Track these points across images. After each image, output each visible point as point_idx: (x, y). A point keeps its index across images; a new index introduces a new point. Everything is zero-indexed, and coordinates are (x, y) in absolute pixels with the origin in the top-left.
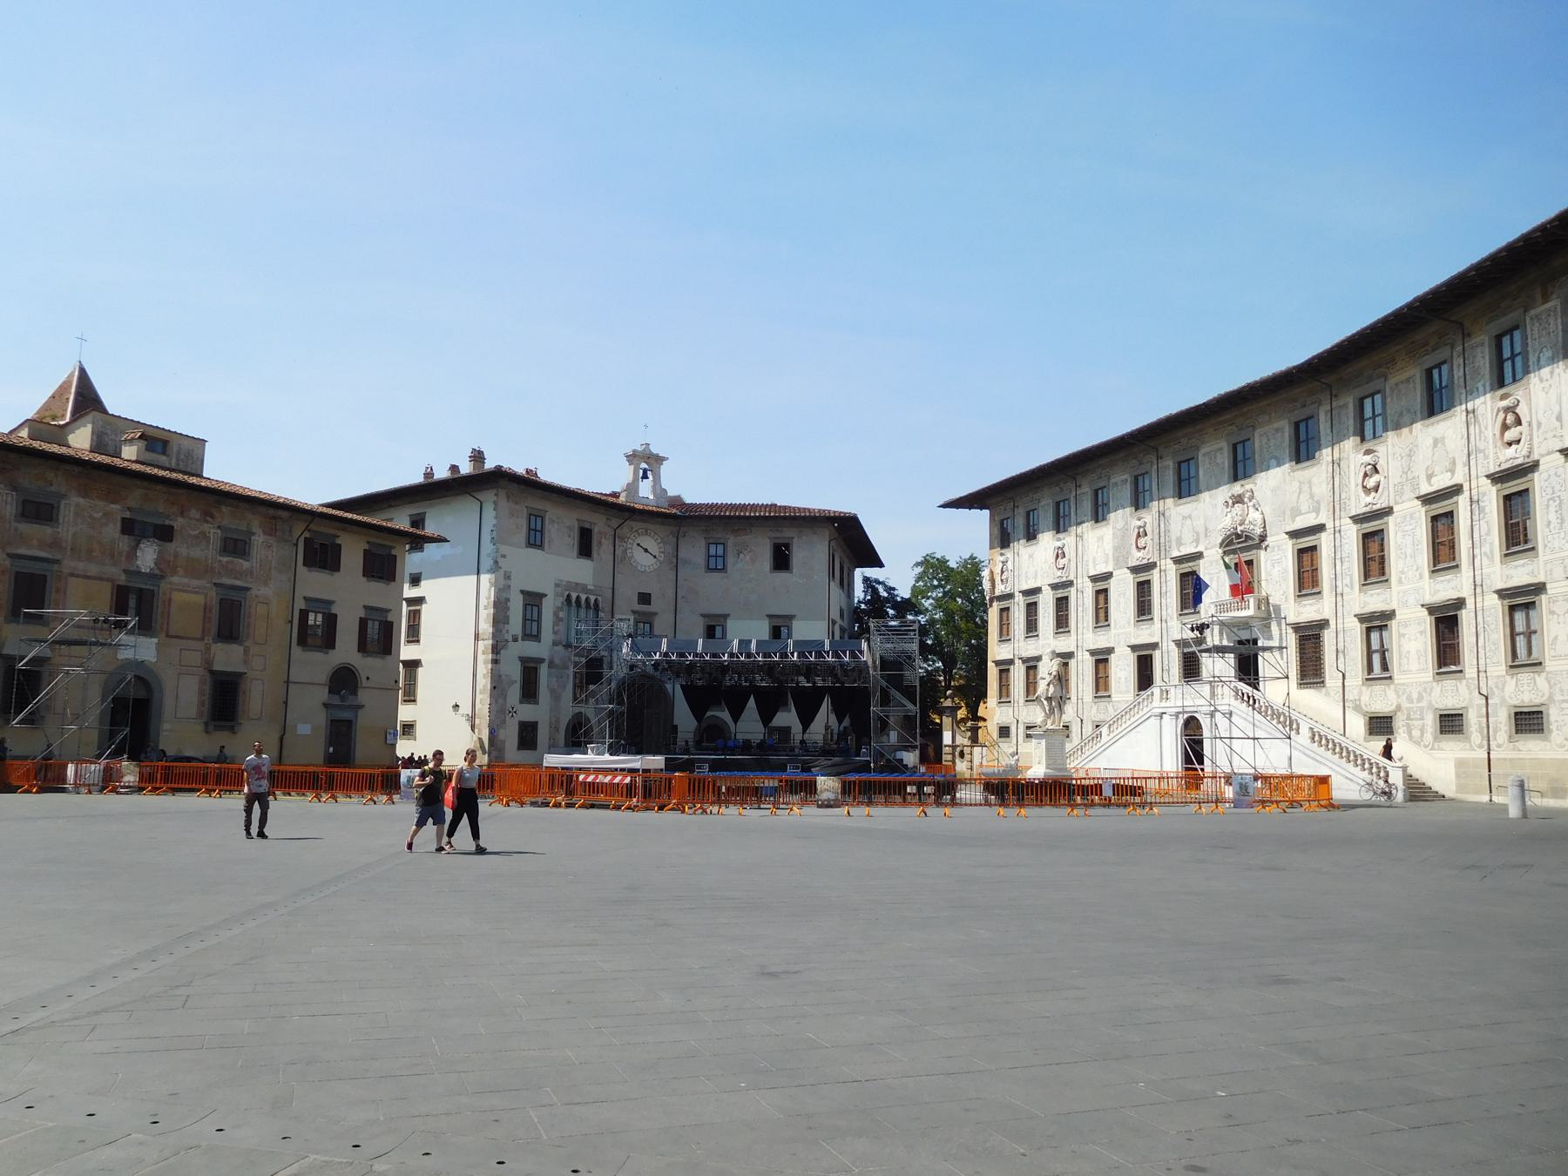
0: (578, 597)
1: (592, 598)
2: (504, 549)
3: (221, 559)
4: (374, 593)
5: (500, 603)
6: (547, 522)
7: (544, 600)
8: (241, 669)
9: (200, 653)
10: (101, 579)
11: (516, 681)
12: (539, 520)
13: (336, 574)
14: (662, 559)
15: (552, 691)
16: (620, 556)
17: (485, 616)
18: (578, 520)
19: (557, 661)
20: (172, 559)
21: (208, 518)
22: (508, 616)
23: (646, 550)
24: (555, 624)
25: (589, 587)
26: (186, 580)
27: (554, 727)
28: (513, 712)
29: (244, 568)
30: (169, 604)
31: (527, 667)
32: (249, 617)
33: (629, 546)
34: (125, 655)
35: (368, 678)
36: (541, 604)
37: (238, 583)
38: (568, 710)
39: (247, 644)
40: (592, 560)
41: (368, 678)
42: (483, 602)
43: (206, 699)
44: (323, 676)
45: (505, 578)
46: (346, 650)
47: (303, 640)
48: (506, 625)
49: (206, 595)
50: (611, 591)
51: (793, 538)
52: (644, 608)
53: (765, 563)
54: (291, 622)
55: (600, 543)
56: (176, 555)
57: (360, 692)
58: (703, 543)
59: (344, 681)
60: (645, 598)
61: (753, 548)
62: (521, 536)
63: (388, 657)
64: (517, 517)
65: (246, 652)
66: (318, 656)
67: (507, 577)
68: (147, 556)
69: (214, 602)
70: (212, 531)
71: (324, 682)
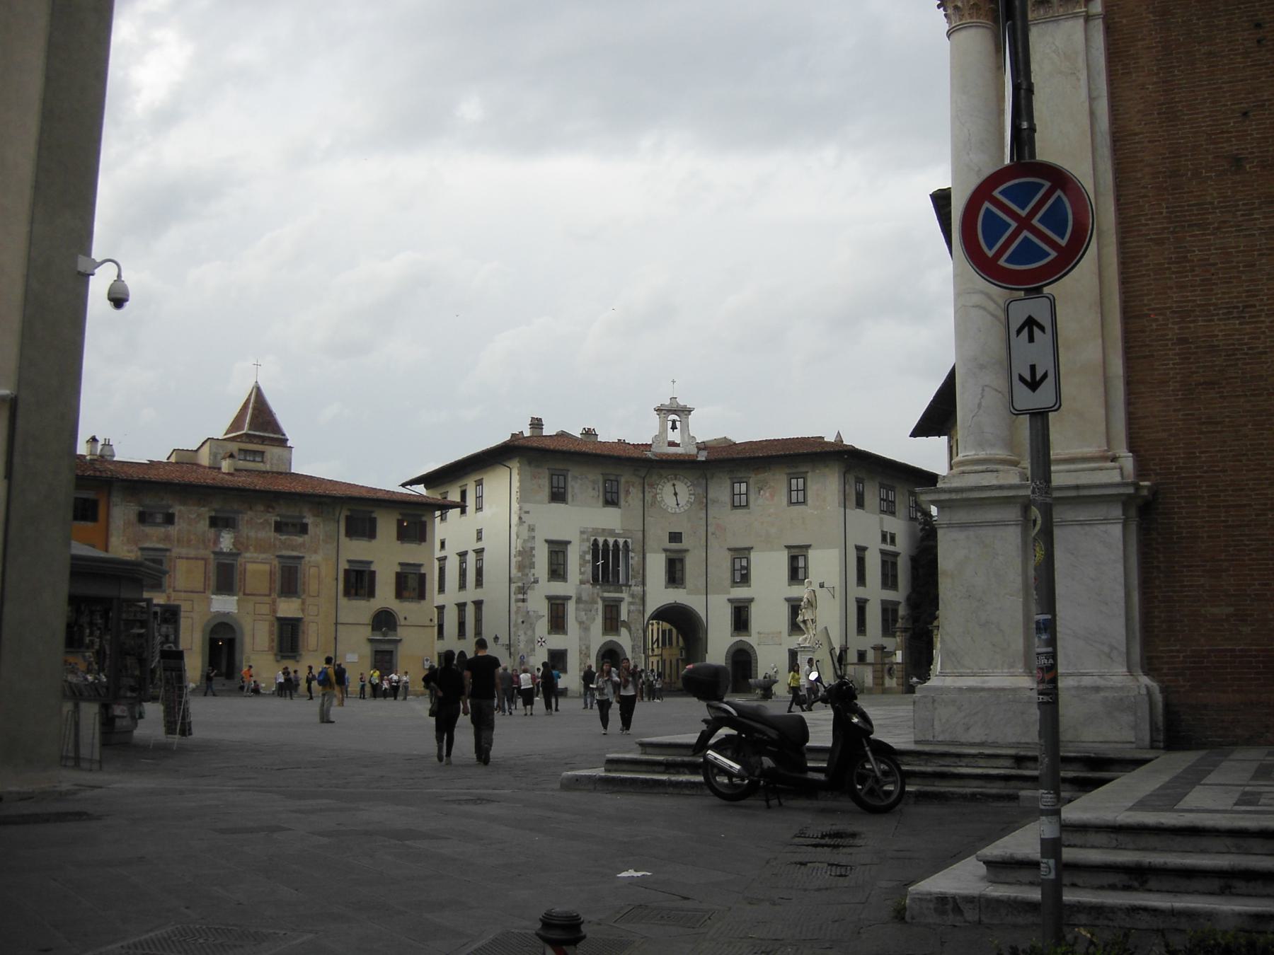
0: (606, 541)
1: (621, 541)
2: (527, 507)
3: (281, 537)
4: (410, 553)
5: (526, 552)
6: (570, 479)
7: (570, 547)
8: (300, 615)
9: (268, 605)
10: (197, 559)
11: (544, 616)
12: (562, 478)
13: (373, 541)
14: (692, 501)
15: (581, 623)
16: (650, 502)
17: (514, 564)
18: (602, 474)
19: (585, 597)
21: (270, 510)
22: (534, 562)
23: (676, 494)
24: (581, 566)
25: (617, 531)
26: (255, 555)
27: (585, 654)
28: (542, 642)
30: (245, 572)
31: (554, 604)
32: (304, 577)
33: (658, 491)
34: (213, 609)
35: (405, 619)
36: (567, 549)
37: (295, 554)
38: (598, 639)
39: (303, 597)
40: (620, 508)
41: (405, 619)
42: (513, 552)
44: (367, 617)
45: (529, 531)
46: (385, 596)
47: (347, 593)
48: (532, 570)
49: (271, 564)
50: (641, 533)
51: (807, 472)
52: (674, 546)
53: (783, 498)
54: (337, 579)
55: (627, 492)
56: (248, 538)
57: (399, 629)
58: (729, 482)
59: (384, 620)
60: (675, 537)
61: (772, 484)
62: (546, 493)
63: (423, 602)
64: (539, 478)
65: (303, 603)
66: (361, 604)
67: (531, 529)
68: (226, 541)
69: (277, 568)
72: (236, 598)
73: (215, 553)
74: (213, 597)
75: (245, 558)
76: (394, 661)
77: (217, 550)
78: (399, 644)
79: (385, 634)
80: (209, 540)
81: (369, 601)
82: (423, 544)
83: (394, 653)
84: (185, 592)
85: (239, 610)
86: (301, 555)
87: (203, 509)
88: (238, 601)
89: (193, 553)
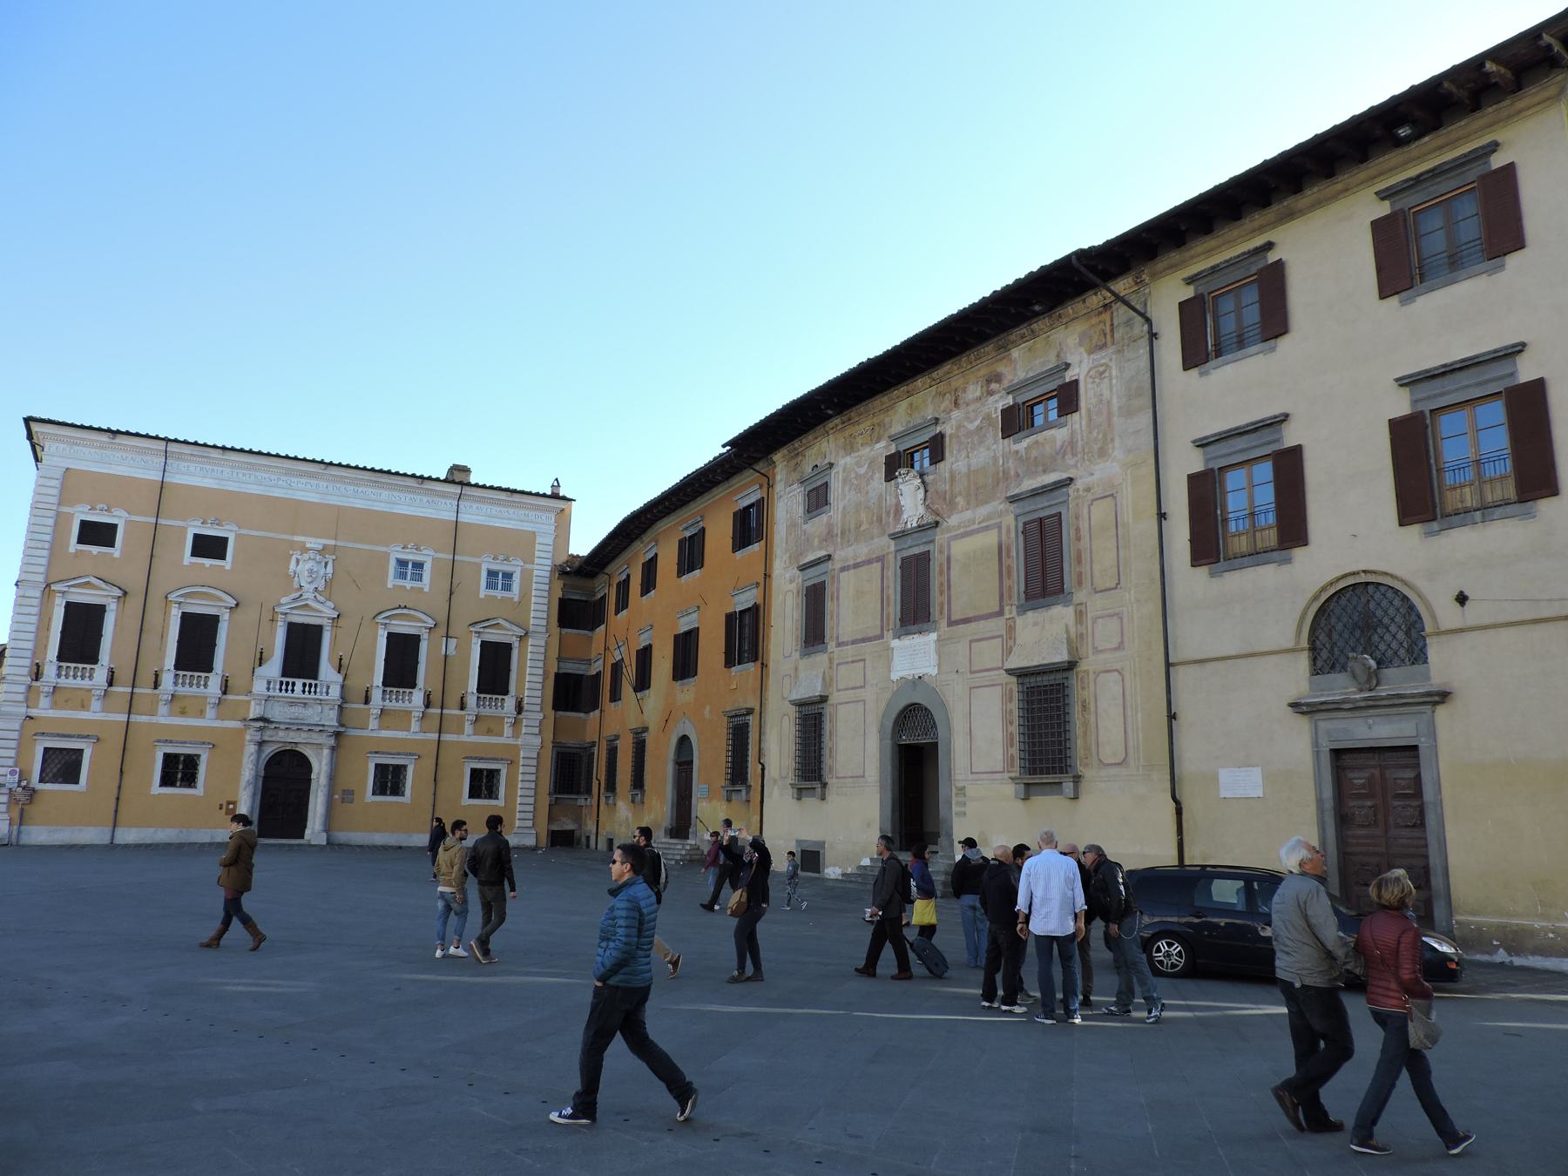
13: (1284, 343)
26: (968, 515)
29: (1059, 444)
35: (1462, 599)
43: (1015, 729)
57: (1436, 651)
65: (1080, 616)
66: (1265, 576)
68: (910, 498)
71: (1291, 645)
72: (933, 636)
73: (895, 537)
74: (895, 643)
75: (949, 530)
76: (1428, 794)
77: (899, 528)
78: (1442, 712)
79: (1373, 679)
80: (888, 513)
81: (1288, 561)
82: (1513, 260)
83: (1424, 752)
85: (939, 666)
86: (1064, 476)
87: (878, 446)
88: (938, 640)
89: (862, 551)
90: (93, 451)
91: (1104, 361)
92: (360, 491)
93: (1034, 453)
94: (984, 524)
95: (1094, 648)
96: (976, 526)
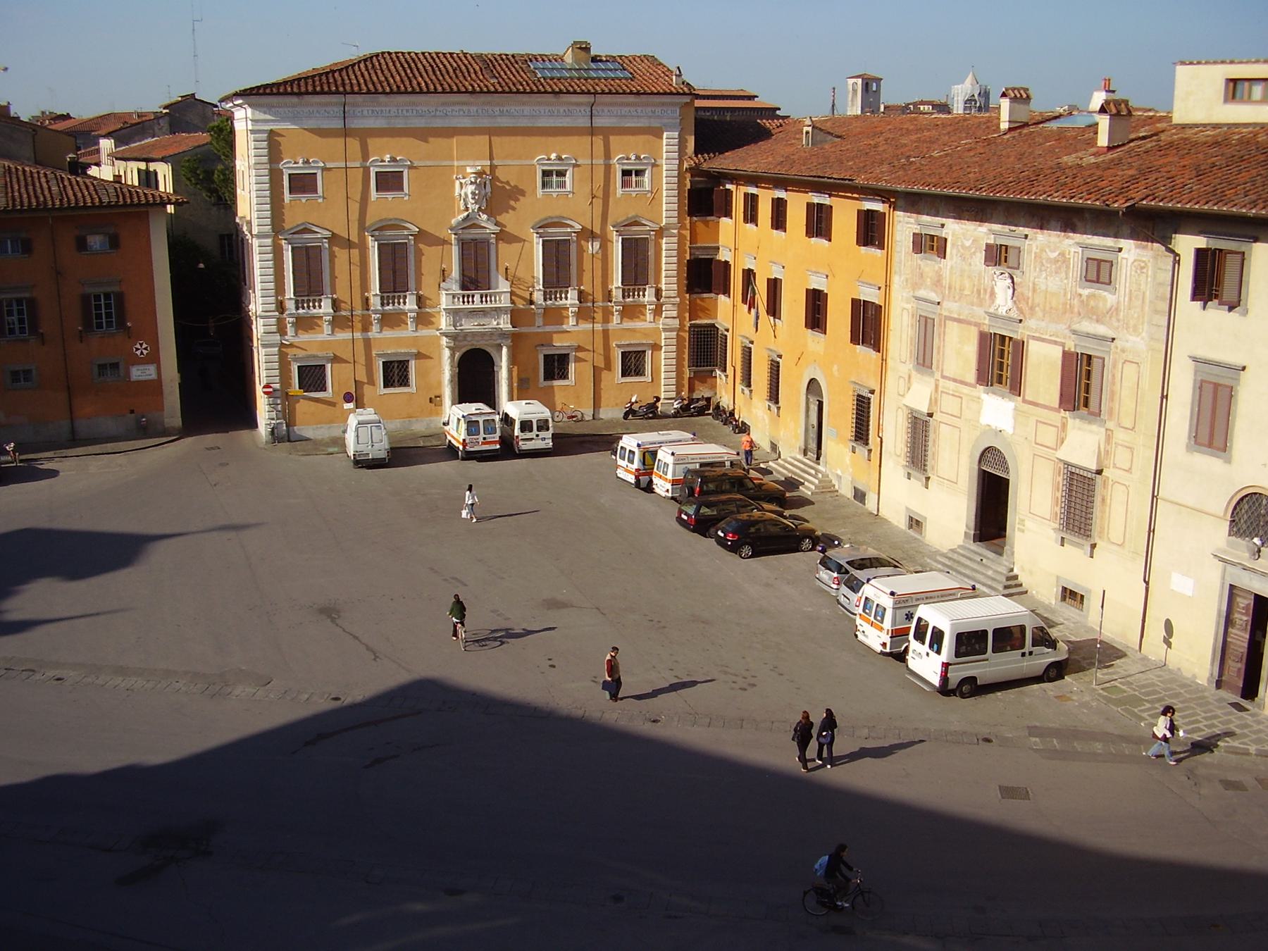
3: (1080, 291)
20: (1030, 295)
26: (1043, 324)
29: (1109, 306)
37: (1101, 330)
39: (1110, 425)
65: (1109, 438)
70: (1073, 250)
77: (991, 310)
84: (955, 380)
85: (1014, 428)
90: (286, 109)
91: (1144, 259)
92: (505, 109)
93: (1092, 303)
94: (1053, 338)
95: (1114, 464)
96: (1047, 337)
